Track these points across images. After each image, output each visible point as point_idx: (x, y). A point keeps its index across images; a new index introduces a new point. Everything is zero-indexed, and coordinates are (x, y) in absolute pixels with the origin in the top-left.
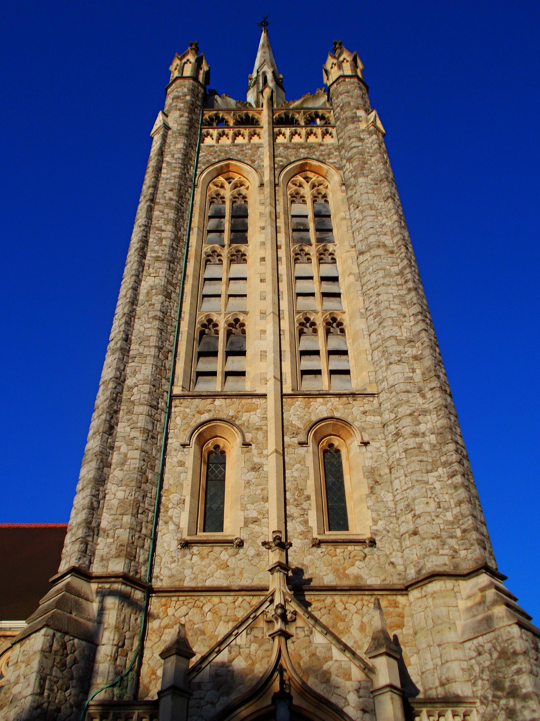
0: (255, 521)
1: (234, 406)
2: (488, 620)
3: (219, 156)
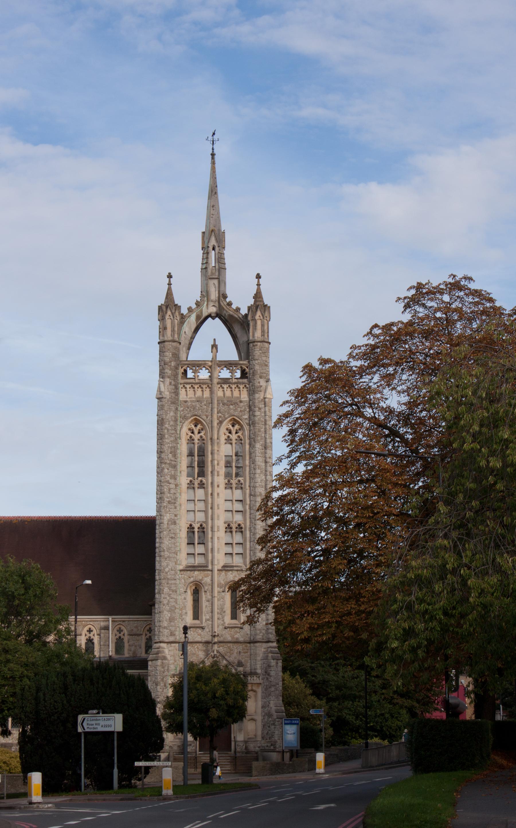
0: (208, 620)
1: (202, 575)
2: (267, 656)
3: (190, 411)
